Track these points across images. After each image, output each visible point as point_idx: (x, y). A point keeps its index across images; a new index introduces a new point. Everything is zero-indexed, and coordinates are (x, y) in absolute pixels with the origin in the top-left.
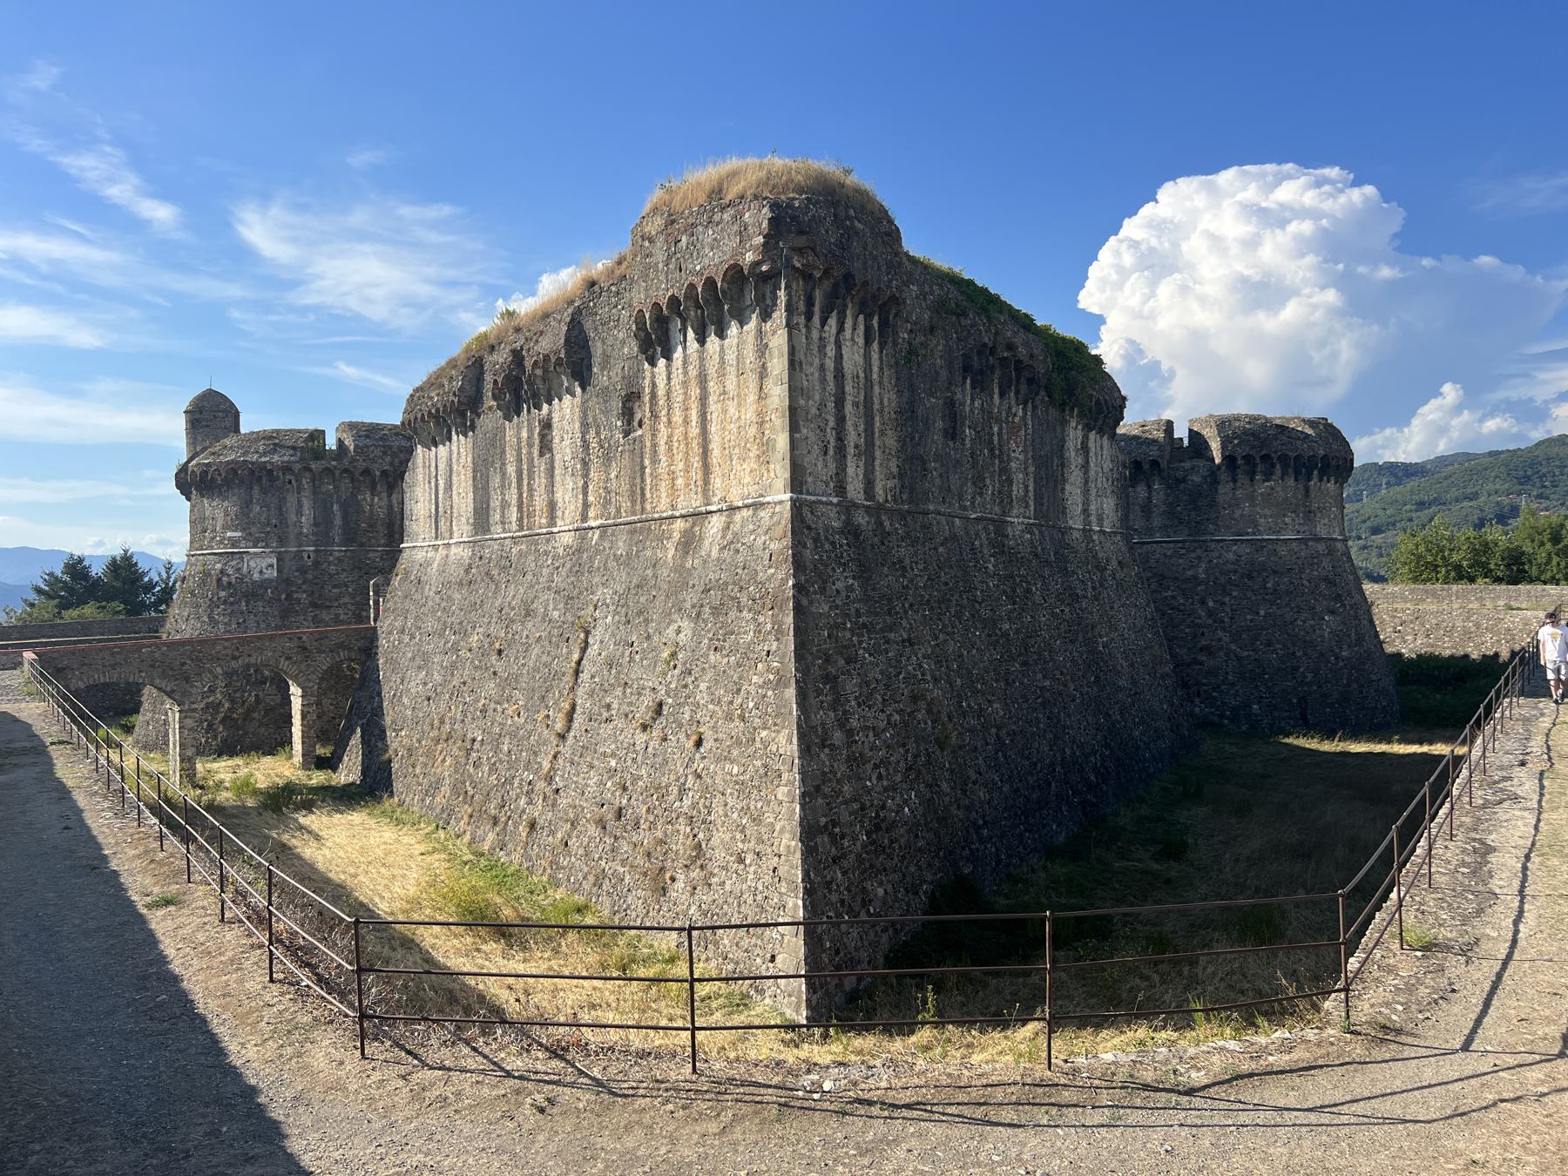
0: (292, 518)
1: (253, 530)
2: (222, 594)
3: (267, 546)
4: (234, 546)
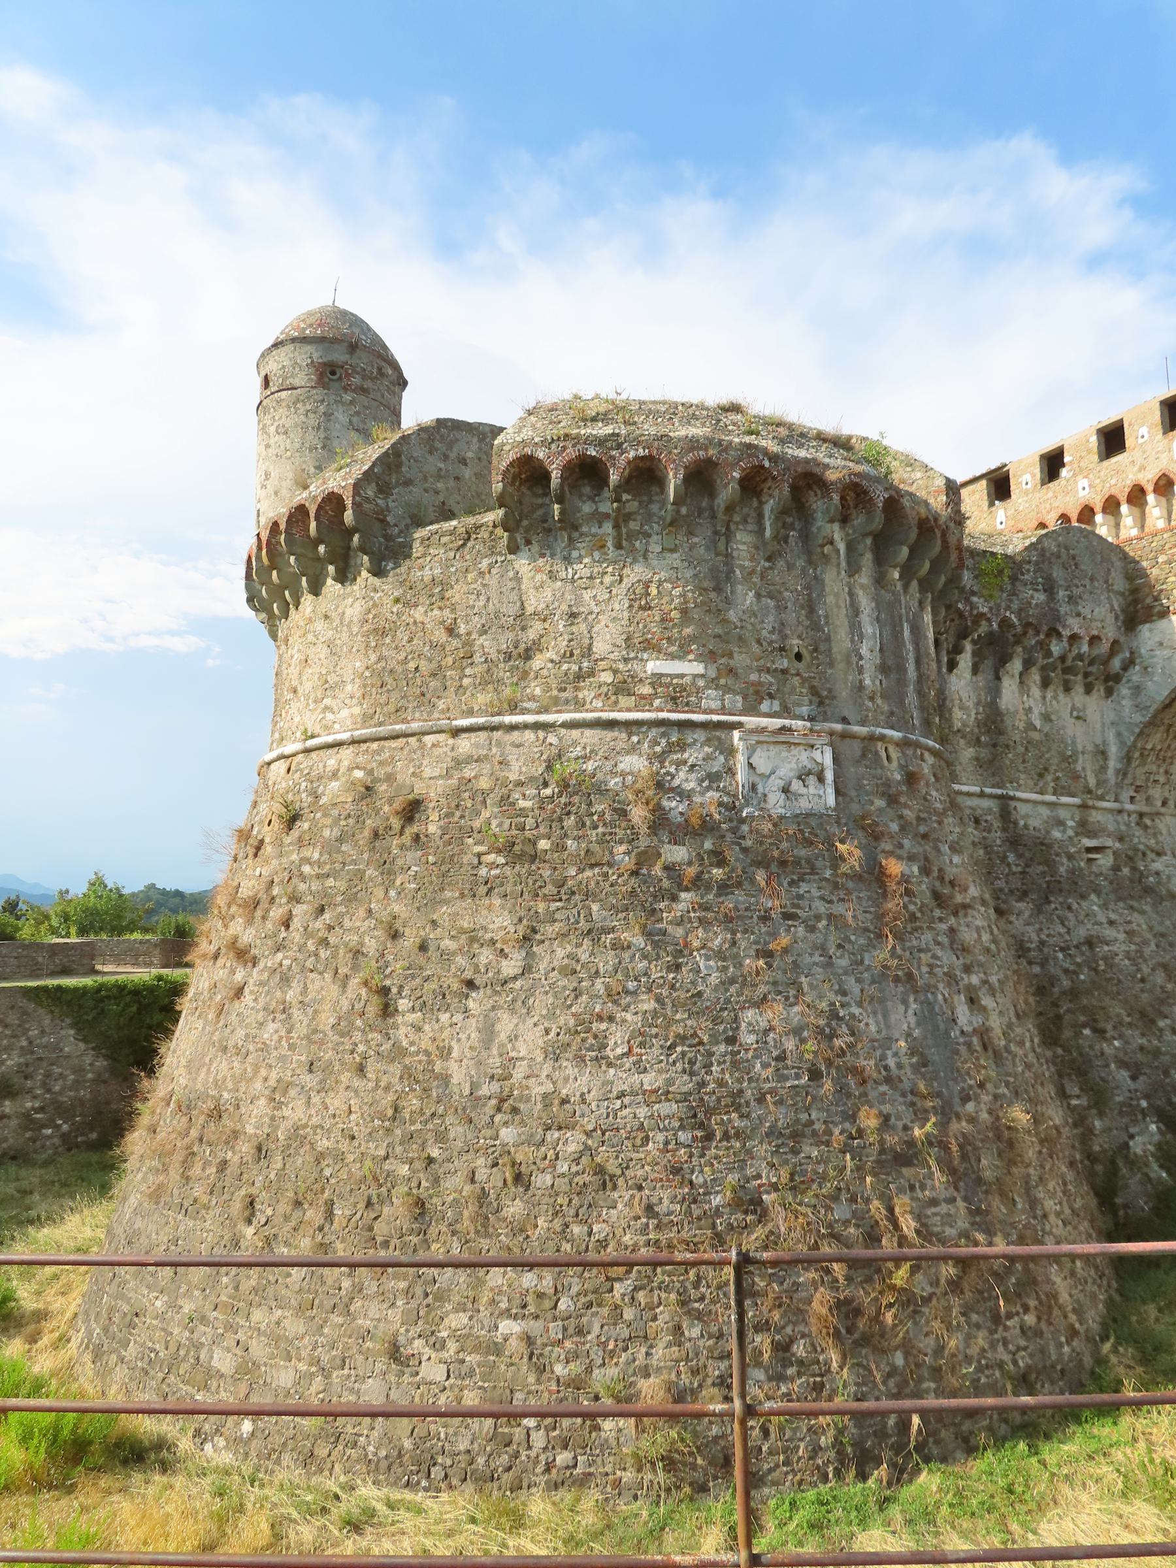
0: (842, 640)
1: (740, 659)
2: (678, 854)
3: (786, 711)
4: (674, 701)
